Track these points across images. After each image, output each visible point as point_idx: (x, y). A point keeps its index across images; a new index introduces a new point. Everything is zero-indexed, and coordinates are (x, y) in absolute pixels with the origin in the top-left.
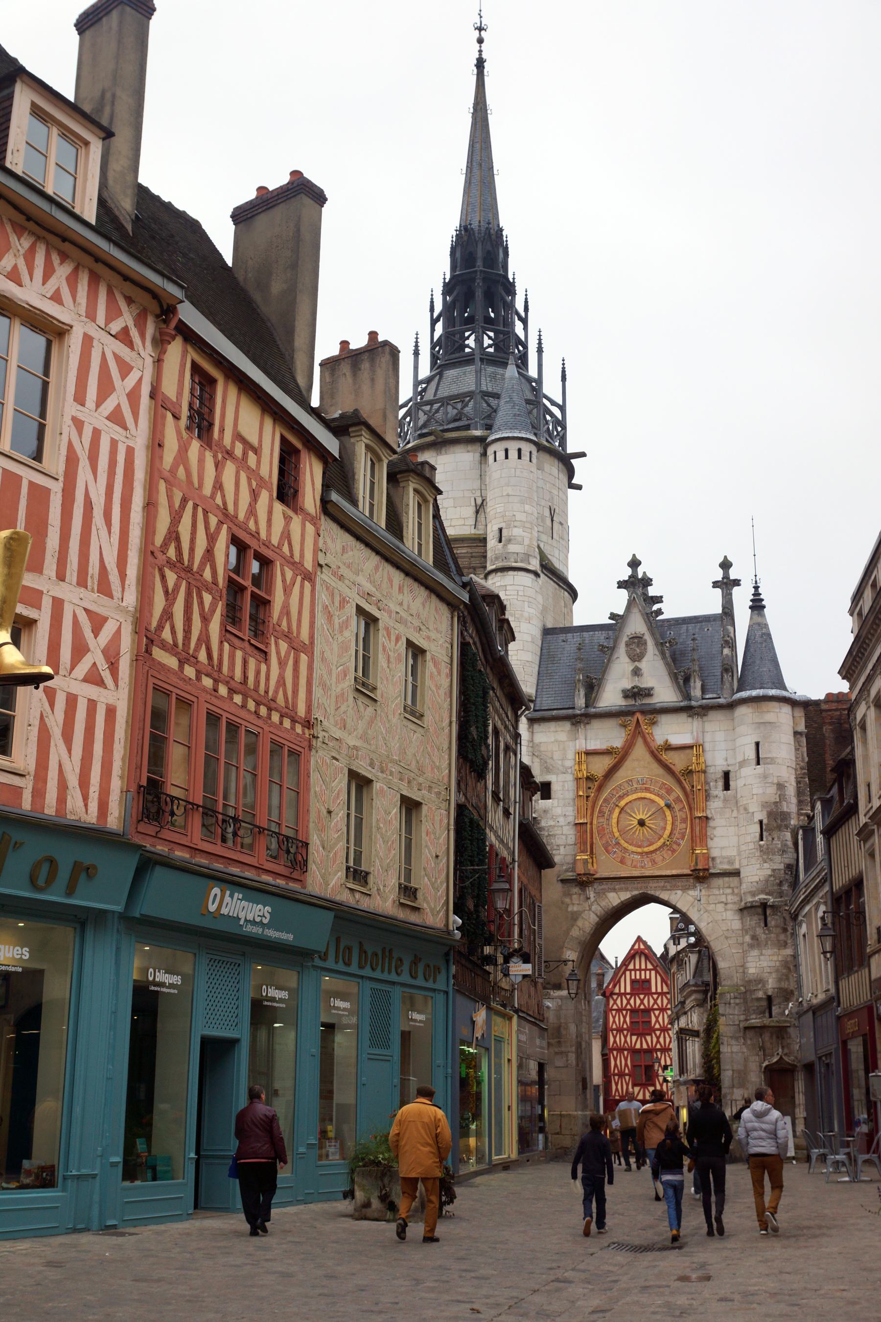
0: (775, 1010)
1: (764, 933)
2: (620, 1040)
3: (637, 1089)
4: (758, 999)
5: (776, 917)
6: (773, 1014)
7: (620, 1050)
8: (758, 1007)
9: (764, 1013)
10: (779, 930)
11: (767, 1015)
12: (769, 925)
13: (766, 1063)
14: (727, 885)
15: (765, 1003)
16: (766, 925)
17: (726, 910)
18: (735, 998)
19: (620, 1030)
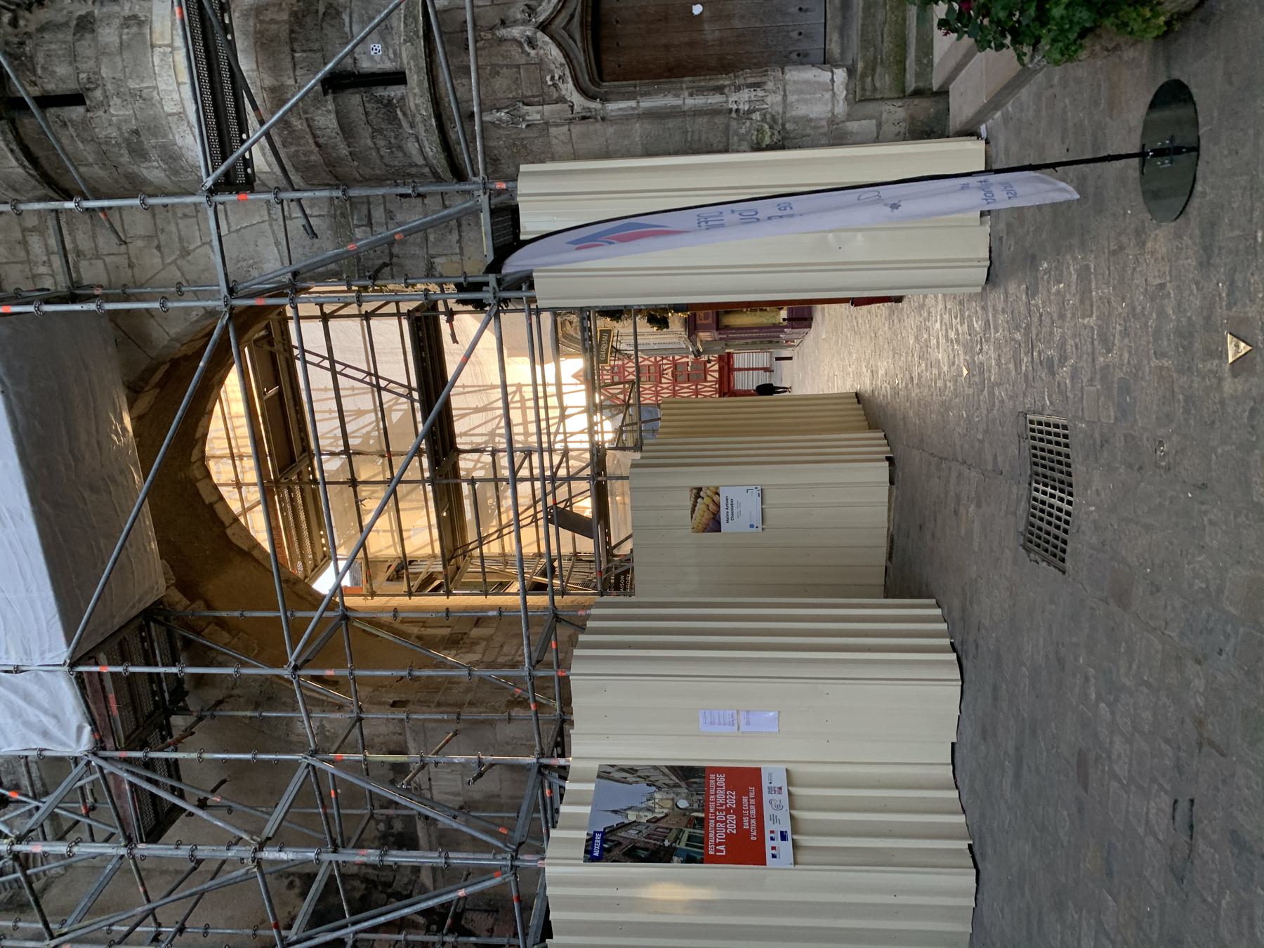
0: (374, 57)
1: (104, 105)
2: (666, 394)
3: (709, 378)
4: (346, 129)
5: (40, 58)
6: (388, 66)
7: (675, 393)
8: (377, 131)
9: (389, 104)
10: (85, 47)
11: (394, 92)
12: (71, 86)
13: (568, 90)
14: (23, 254)
15: (354, 100)
16: (76, 99)
17: (98, 256)
18: (370, 224)
19: (657, 394)
